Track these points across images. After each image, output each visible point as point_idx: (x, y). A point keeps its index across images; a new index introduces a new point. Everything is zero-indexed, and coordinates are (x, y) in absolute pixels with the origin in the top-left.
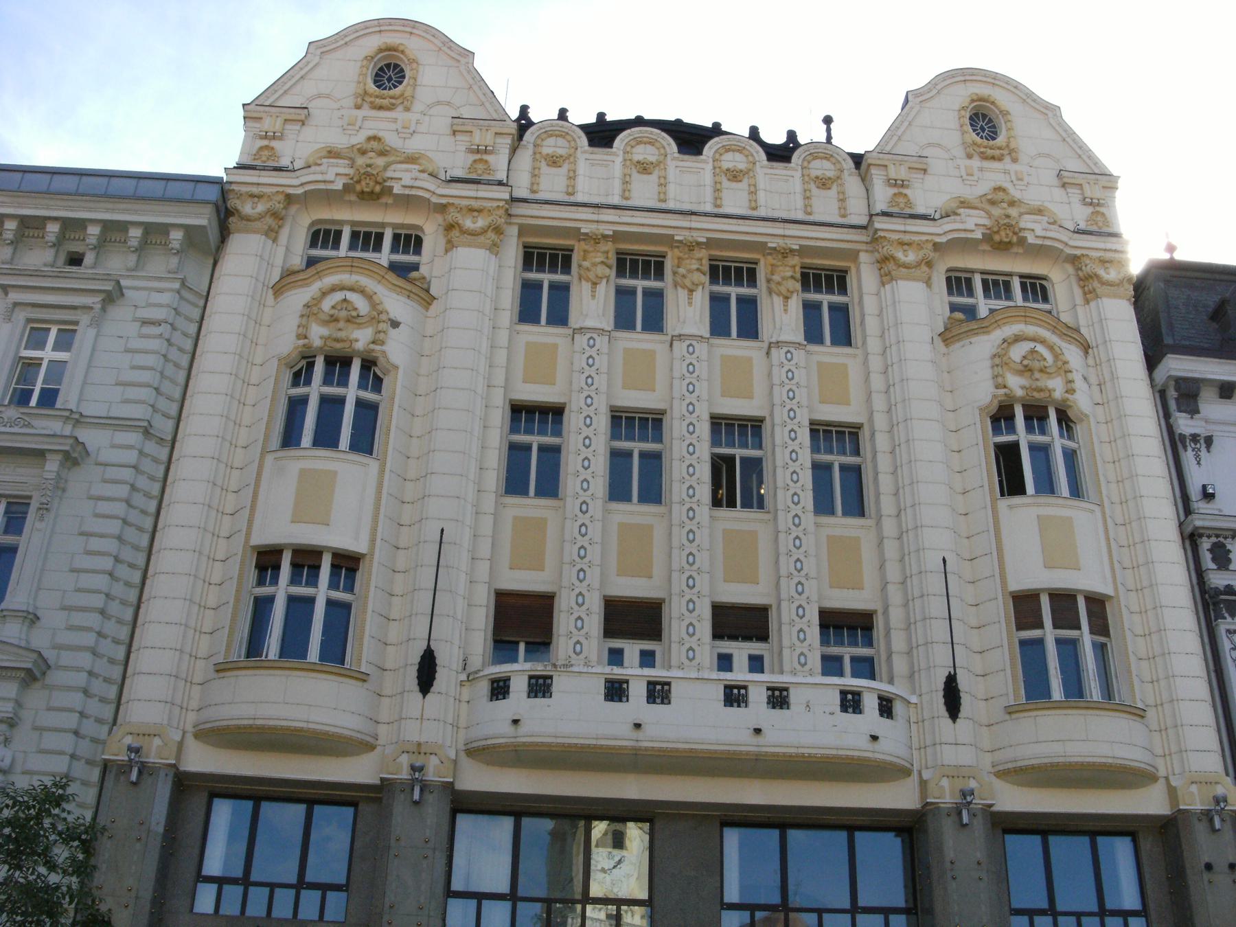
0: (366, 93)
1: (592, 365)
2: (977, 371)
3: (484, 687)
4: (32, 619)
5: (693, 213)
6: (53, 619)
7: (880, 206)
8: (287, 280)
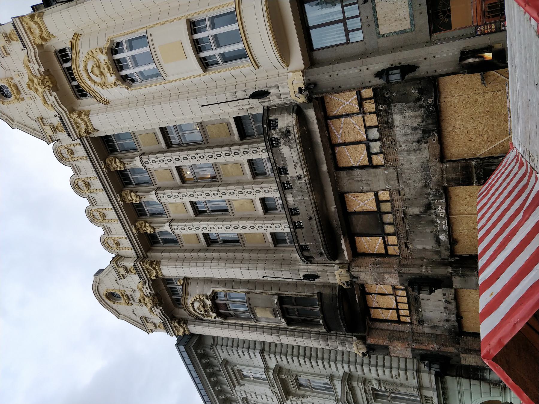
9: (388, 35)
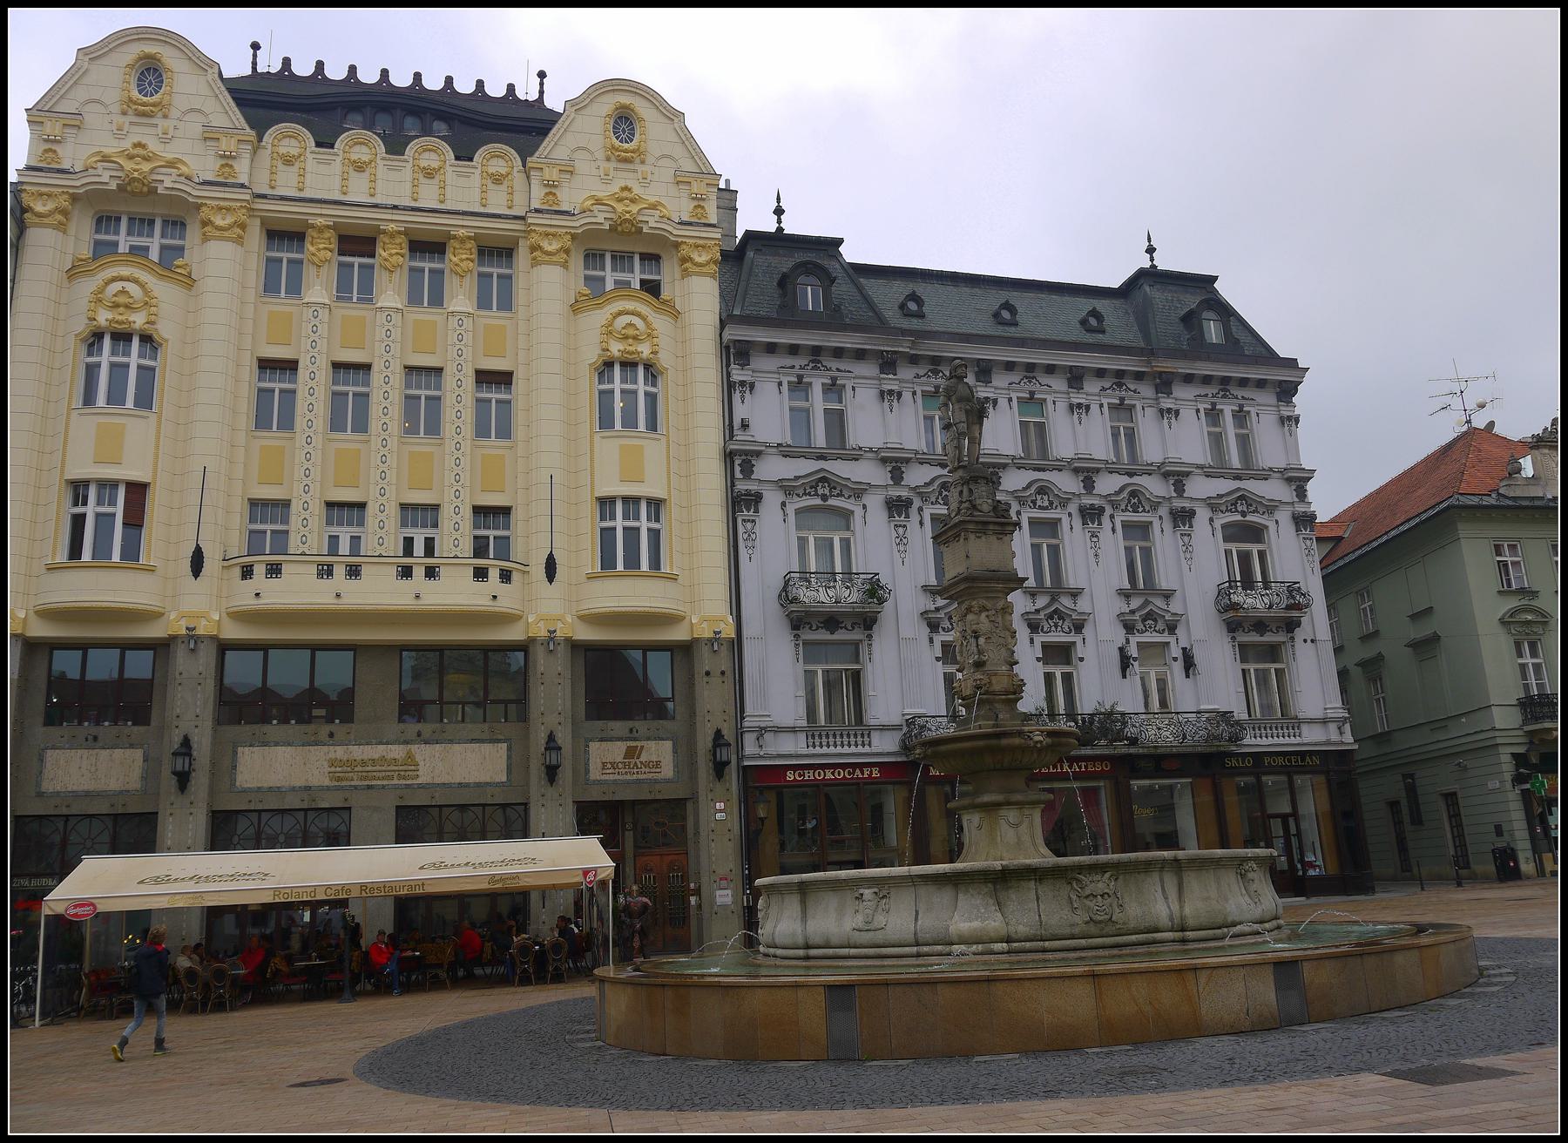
0: (130, 100)
2: (592, 335)
3: (237, 572)
5: (395, 207)
7: (536, 204)
8: (74, 272)
9: (587, 752)
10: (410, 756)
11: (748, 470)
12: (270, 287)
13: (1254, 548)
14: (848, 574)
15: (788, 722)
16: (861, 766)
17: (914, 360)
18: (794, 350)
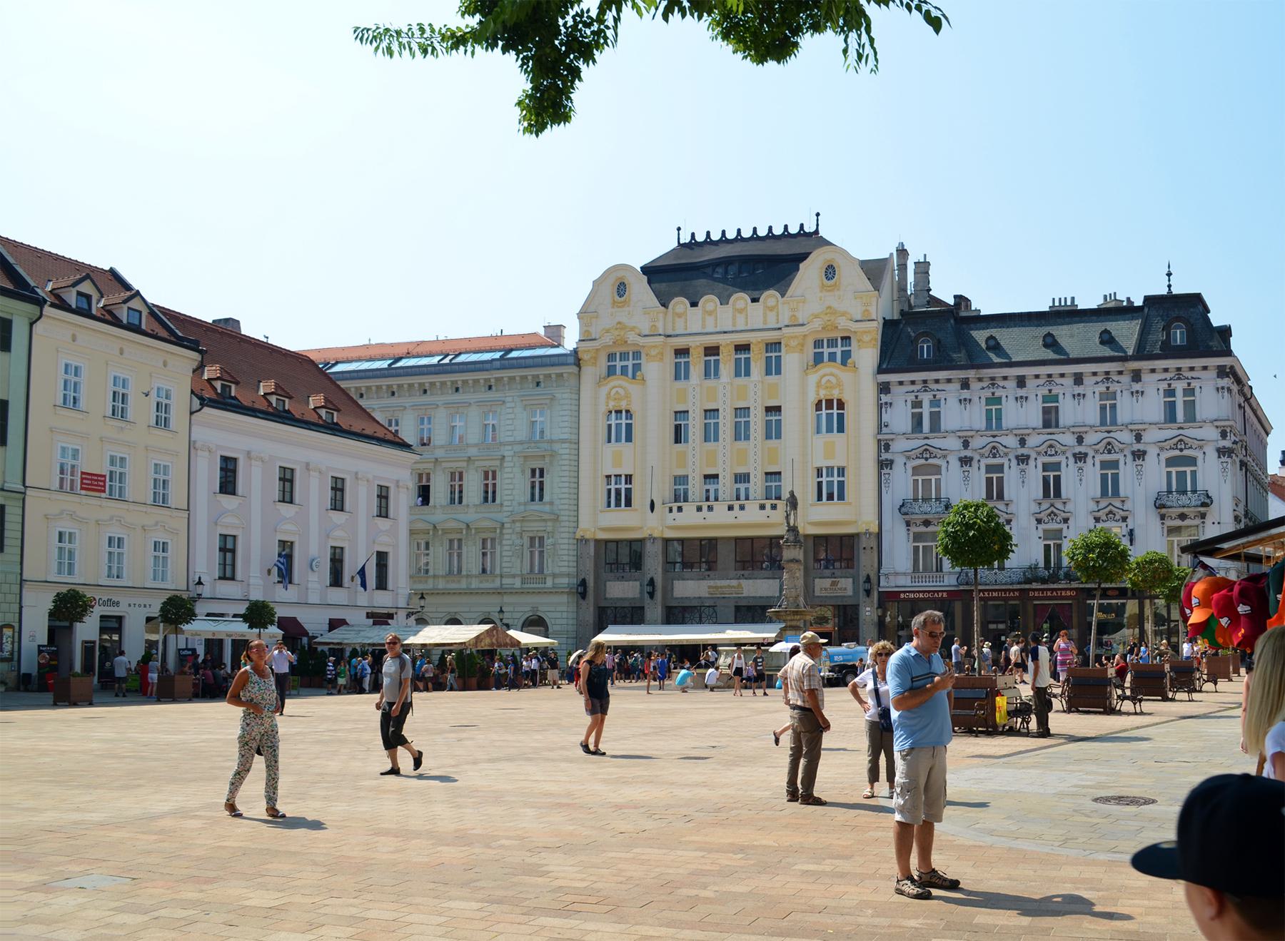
1: (697, 393)
4: (551, 503)
6: (557, 502)
8: (600, 382)
10: (739, 585)
11: (887, 447)
12: (677, 377)
13: (1188, 469)
14: (938, 499)
15: (902, 570)
16: (938, 592)
17: (980, 380)
18: (913, 383)
